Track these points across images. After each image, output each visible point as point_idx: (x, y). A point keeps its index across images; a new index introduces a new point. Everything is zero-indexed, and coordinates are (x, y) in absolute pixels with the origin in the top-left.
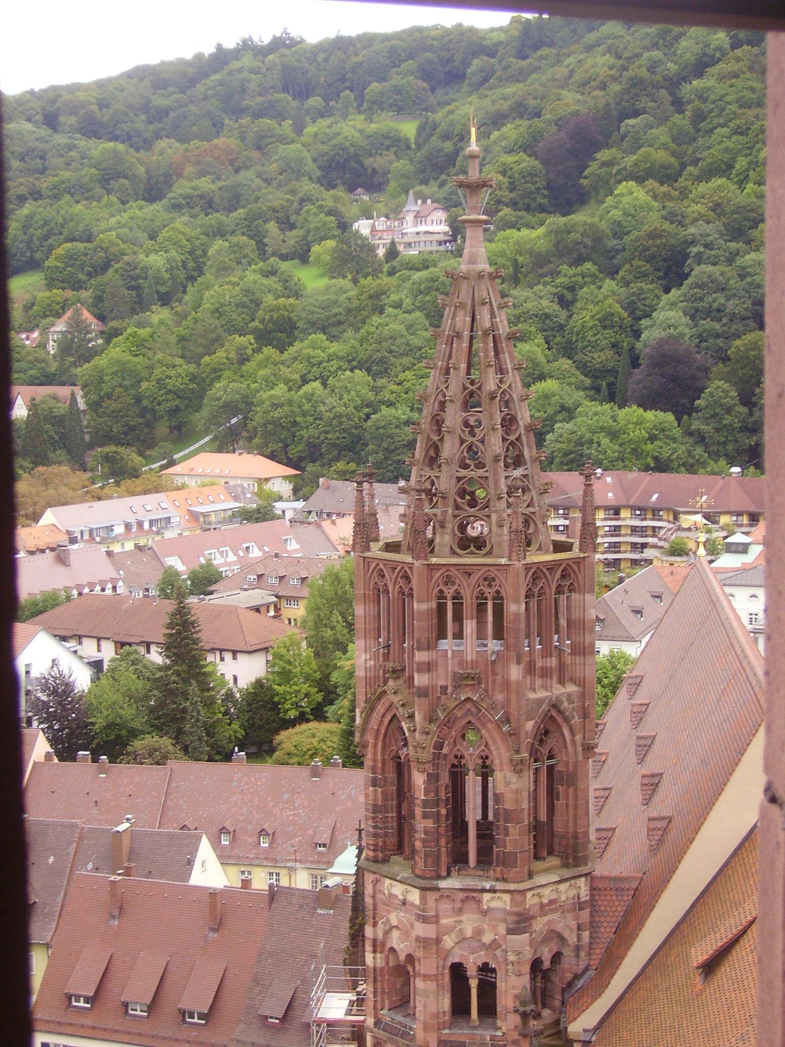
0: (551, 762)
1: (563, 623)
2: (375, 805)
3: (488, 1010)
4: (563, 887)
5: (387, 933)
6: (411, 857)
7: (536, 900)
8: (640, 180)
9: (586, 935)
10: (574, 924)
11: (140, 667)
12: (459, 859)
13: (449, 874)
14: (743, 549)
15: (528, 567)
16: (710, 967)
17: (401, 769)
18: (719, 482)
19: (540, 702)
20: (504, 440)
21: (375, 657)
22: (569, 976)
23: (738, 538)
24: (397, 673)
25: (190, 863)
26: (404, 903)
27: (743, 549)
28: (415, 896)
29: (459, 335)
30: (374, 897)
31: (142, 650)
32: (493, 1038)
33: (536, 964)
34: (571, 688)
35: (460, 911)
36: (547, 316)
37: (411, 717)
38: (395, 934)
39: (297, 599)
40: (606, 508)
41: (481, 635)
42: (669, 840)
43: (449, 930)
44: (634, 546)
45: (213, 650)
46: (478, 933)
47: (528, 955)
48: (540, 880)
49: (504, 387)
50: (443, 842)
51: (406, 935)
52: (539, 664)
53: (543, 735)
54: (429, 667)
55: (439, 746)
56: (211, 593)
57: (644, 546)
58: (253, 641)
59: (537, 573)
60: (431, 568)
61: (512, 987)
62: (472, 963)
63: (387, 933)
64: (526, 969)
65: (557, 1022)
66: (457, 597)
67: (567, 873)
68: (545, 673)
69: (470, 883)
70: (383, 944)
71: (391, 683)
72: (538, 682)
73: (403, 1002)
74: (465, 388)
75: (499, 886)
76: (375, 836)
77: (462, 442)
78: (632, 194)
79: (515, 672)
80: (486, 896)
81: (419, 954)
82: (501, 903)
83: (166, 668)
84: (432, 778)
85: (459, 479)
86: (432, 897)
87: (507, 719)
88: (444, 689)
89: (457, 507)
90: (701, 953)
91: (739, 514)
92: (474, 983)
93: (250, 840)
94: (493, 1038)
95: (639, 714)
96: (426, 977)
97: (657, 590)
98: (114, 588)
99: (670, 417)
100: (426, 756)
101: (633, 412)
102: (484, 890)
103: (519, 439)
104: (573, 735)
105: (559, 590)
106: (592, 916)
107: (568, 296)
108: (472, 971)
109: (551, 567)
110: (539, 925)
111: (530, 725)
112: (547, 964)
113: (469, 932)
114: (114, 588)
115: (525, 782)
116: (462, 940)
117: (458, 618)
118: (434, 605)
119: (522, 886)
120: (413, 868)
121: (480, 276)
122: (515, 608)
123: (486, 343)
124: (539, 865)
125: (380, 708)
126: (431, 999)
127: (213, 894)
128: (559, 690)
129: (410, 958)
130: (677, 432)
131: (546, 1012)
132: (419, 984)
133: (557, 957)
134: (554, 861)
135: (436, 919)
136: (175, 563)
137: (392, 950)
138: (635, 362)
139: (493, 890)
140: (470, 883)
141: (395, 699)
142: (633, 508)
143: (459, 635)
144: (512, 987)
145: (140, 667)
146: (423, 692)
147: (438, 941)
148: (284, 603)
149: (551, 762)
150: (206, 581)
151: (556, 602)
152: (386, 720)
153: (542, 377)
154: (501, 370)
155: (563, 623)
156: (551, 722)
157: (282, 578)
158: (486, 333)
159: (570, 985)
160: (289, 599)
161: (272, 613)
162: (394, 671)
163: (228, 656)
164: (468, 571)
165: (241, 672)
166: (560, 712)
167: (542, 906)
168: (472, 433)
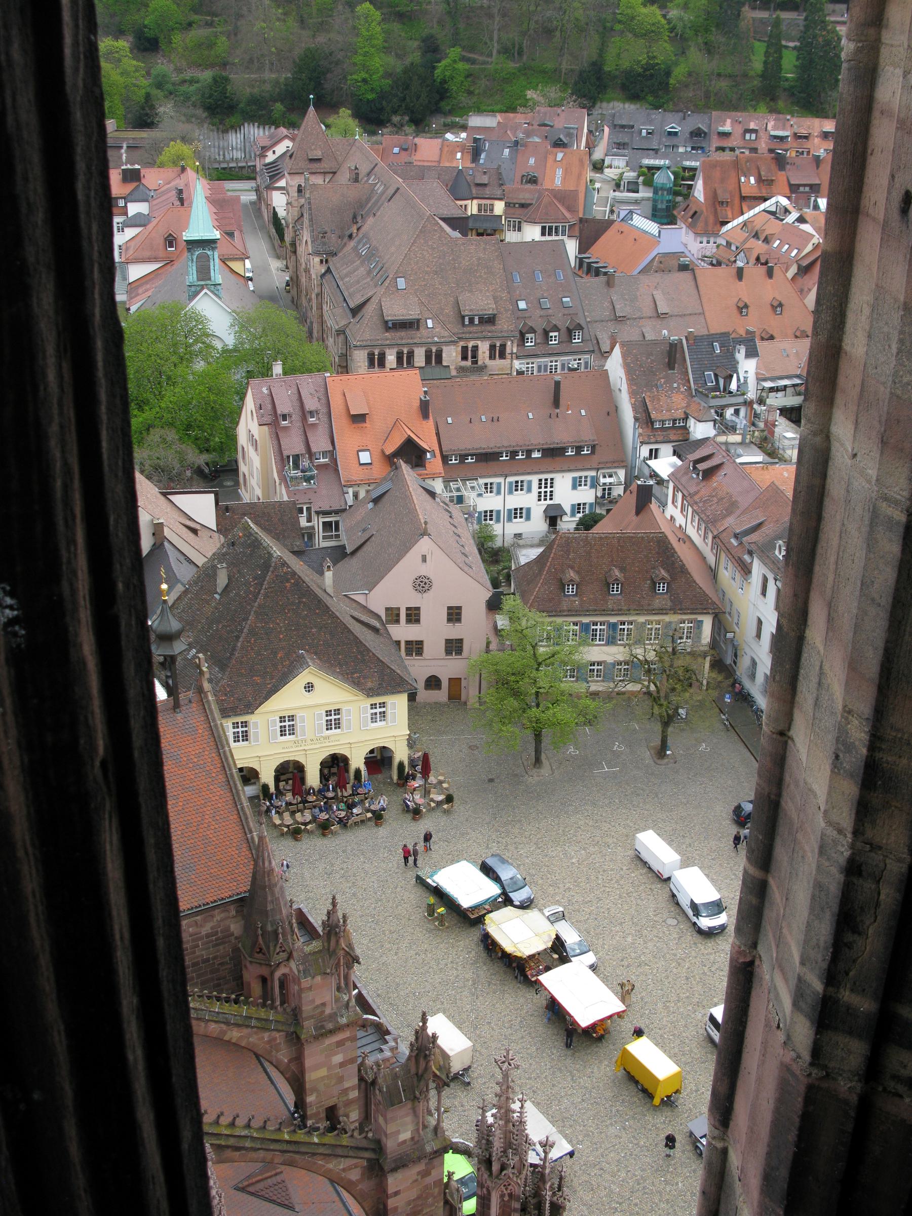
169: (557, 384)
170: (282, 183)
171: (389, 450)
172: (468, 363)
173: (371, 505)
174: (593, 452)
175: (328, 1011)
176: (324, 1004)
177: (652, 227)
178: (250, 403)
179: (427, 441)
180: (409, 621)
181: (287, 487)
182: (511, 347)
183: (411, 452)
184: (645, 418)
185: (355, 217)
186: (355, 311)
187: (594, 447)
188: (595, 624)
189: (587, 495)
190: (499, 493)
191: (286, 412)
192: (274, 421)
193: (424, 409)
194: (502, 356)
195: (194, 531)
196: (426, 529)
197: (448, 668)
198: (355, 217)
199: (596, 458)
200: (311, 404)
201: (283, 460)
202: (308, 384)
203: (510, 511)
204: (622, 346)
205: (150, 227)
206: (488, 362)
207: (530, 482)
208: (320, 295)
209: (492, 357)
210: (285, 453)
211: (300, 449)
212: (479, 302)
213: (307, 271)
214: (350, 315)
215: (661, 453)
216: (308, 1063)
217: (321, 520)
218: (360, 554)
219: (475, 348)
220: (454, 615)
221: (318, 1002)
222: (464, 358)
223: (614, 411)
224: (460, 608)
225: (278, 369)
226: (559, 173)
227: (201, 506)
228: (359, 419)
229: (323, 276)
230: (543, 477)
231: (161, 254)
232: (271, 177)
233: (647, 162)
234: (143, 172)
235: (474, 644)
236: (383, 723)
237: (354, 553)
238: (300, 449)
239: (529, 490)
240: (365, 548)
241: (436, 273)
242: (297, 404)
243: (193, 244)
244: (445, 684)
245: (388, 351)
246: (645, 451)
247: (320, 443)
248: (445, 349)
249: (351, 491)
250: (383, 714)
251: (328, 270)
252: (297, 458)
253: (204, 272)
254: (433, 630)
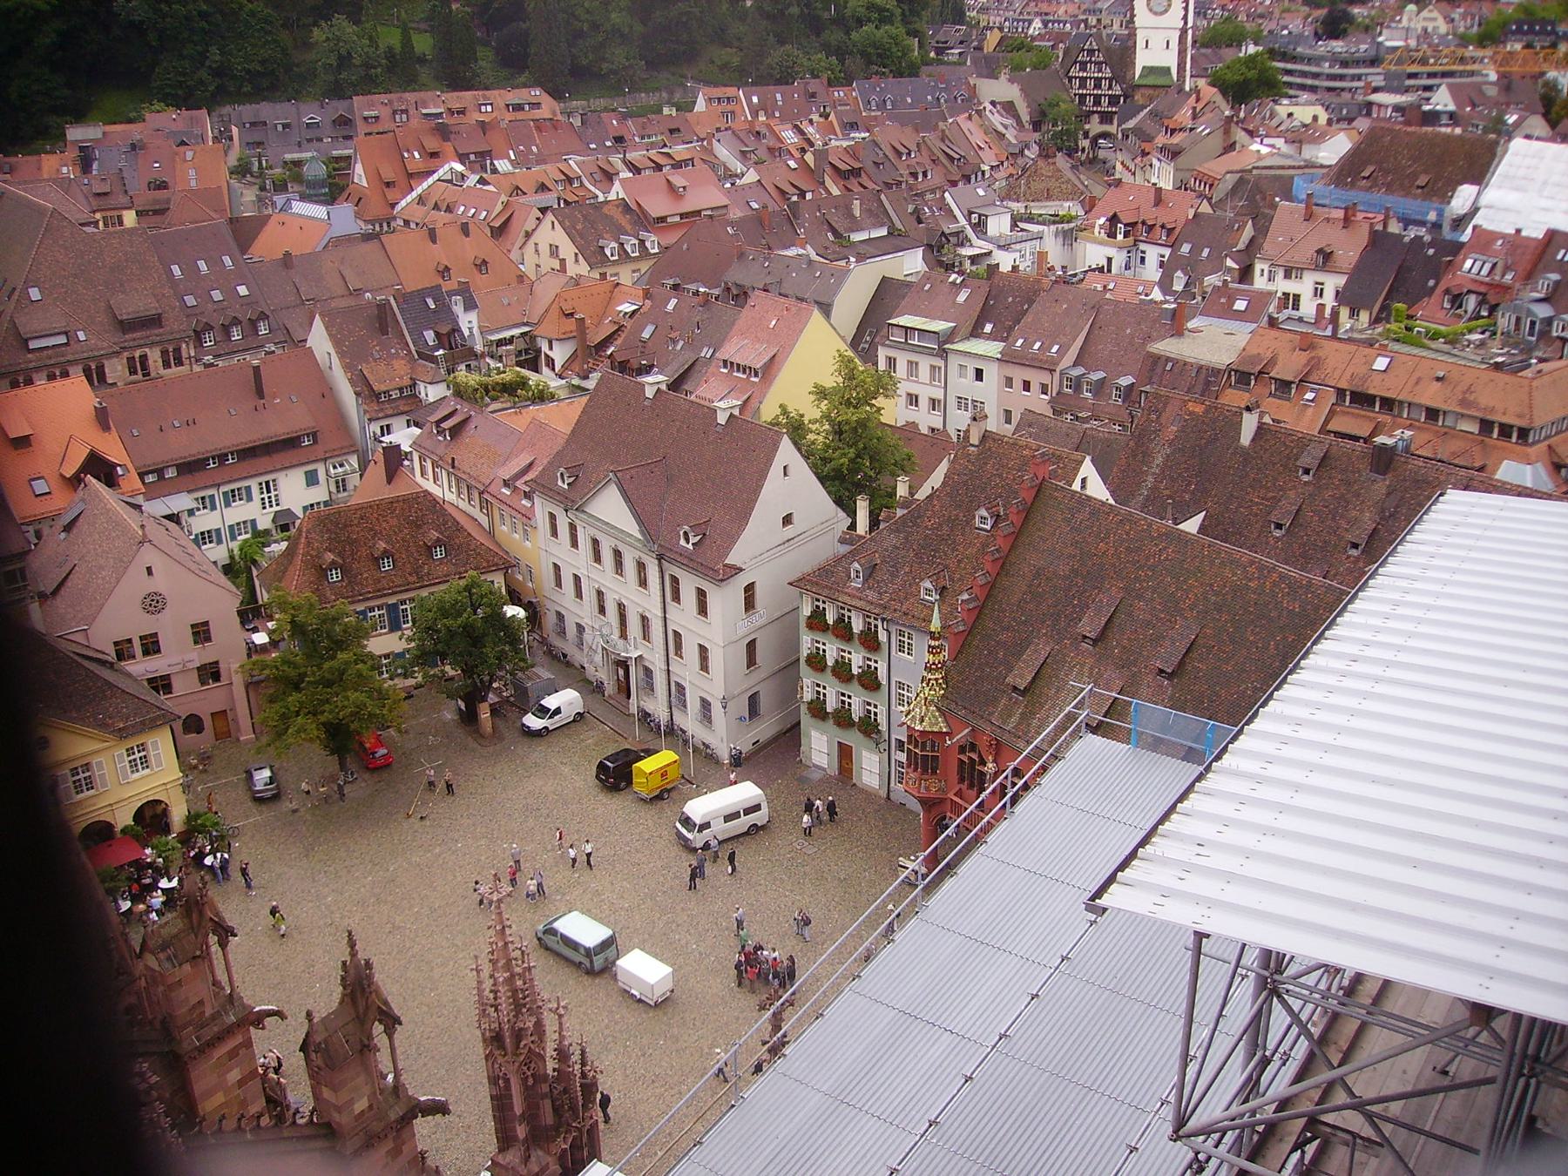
169: (256, 369)
171: (69, 472)
172: (140, 376)
173: (63, 535)
174: (315, 441)
175: (208, 1012)
176: (201, 1003)
177: (319, 211)
179: (114, 451)
180: (146, 653)
182: (188, 350)
183: (100, 468)
184: (368, 393)
187: (314, 435)
188: (372, 609)
189: (319, 494)
190: (213, 508)
193: (102, 418)
194: (179, 363)
196: (144, 535)
197: (207, 702)
199: (320, 450)
203: (231, 527)
204: (322, 316)
206: (162, 372)
207: (248, 489)
209: (167, 365)
212: (135, 304)
215: (394, 428)
216: (198, 1088)
219: (144, 358)
220: (201, 633)
221: (194, 1001)
222: (133, 371)
223: (327, 392)
224: (206, 623)
226: (192, 172)
230: (263, 479)
233: (288, 157)
235: (233, 665)
236: (147, 771)
239: (250, 499)
241: (75, 276)
244: (208, 722)
245: (34, 376)
246: (375, 428)
248: (106, 363)
250: (145, 761)
254: (178, 656)
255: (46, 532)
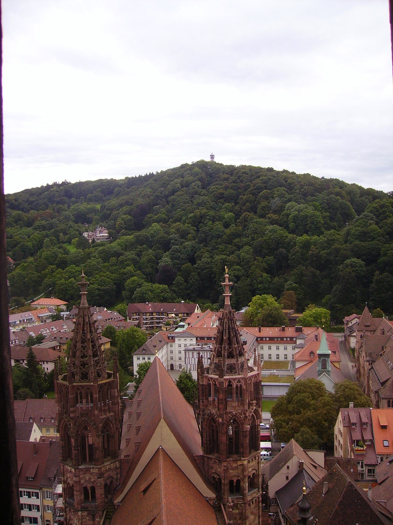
0: (107, 433)
1: (109, 397)
2: (62, 446)
3: (94, 497)
4: (112, 465)
5: (67, 479)
6: (72, 459)
7: (105, 469)
8: (158, 222)
9: (119, 476)
10: (115, 473)
11: (20, 368)
12: (84, 460)
13: (82, 464)
14: (183, 326)
15: (99, 385)
16: (145, 491)
17: (69, 438)
18: (178, 305)
19: (104, 418)
20: (92, 350)
21: (61, 408)
22: (115, 486)
23: (182, 323)
24: (66, 413)
25: (31, 431)
26: (71, 471)
27: (183, 326)
28: (73, 470)
29: (80, 324)
30: (63, 470)
31: (21, 362)
32: (95, 505)
33: (106, 485)
34: (112, 414)
35: (85, 474)
36: (134, 259)
37: (70, 424)
38: (69, 479)
39: (65, 344)
40: (149, 313)
41: (87, 402)
42: (140, 448)
43: (82, 479)
44: (157, 322)
45: (41, 361)
46: (90, 479)
47: (103, 483)
48: (106, 464)
49: (92, 336)
50: (80, 456)
51: (72, 480)
52: (103, 408)
53: (104, 427)
54: (73, 412)
55: (77, 432)
56: (42, 343)
57: (160, 322)
58: (52, 358)
59: (101, 386)
60: (74, 386)
61: (100, 492)
62: (89, 486)
63: (67, 479)
64: (103, 487)
65: (112, 499)
66: (81, 393)
67: (113, 461)
68: (105, 411)
69: (87, 466)
70: (66, 481)
71: (65, 415)
72: (103, 413)
73: (72, 496)
74: (82, 337)
75: (95, 467)
76: (63, 454)
77: (82, 352)
78: (156, 226)
79: (96, 412)
80: (91, 470)
81: (75, 485)
82: (96, 471)
83: (27, 369)
84: (76, 440)
85: (81, 361)
86: (77, 471)
87: (95, 424)
88: (78, 417)
89: (81, 369)
90: (142, 487)
91: (184, 313)
92: (90, 491)
93: (48, 420)
94: (95, 505)
95: (139, 403)
96: (77, 491)
97: (160, 340)
98: (15, 342)
99: (166, 286)
100: (74, 435)
101: (156, 285)
102: (91, 468)
103: (97, 350)
104: (113, 425)
105: (108, 389)
106: (120, 470)
107: (140, 254)
108: (89, 488)
109: (105, 384)
110: (106, 475)
111: (101, 425)
112: (109, 484)
113: (88, 479)
114: (15, 342)
115: (101, 439)
116: (86, 481)
117: (81, 398)
118: (75, 395)
119: (100, 466)
120: (73, 462)
121: (85, 308)
122: (96, 396)
123: (87, 325)
124: (105, 459)
125: (62, 422)
126: (78, 496)
127: (34, 444)
128: (109, 415)
129: (73, 485)
130: (168, 290)
131: (109, 496)
132: (75, 493)
133: (111, 482)
134: (110, 458)
135: (79, 476)
136: (32, 334)
137: (68, 483)
138: (157, 271)
139: (93, 468)
140: (87, 466)
141: (66, 420)
142: (156, 313)
143: (81, 402)
144: (100, 492)
145: (20, 368)
146: (72, 418)
147: (80, 481)
148: (62, 345)
149: (107, 433)
150: (40, 339)
151: (107, 392)
152: (64, 424)
153: (133, 276)
154: (91, 332)
155: (109, 397)
156: (107, 423)
157: (61, 338)
158: (87, 323)
159: (115, 489)
160: (63, 344)
161: (58, 348)
162: (65, 412)
163: (45, 363)
164: (83, 387)
165: (49, 367)
166: (109, 420)
167: (106, 470)
168: (84, 349)
170: (355, 334)
173: (388, 464)
178: (340, 418)
181: (353, 453)
185: (383, 347)
186: (383, 384)
191: (354, 422)
192: (349, 426)
195: (315, 467)
198: (383, 347)
200: (364, 420)
201: (352, 442)
202: (363, 412)
205: (304, 349)
208: (368, 377)
210: (353, 439)
211: (359, 438)
213: (364, 368)
214: (380, 385)
217: (367, 468)
218: (383, 484)
225: (351, 405)
227: (319, 457)
228: (384, 427)
229: (370, 370)
231: (308, 358)
232: (350, 332)
234: (303, 328)
237: (380, 484)
238: (359, 438)
240: (385, 482)
242: (359, 419)
243: (320, 356)
247: (367, 436)
249: (380, 457)
251: (372, 368)
252: (358, 441)
253: (324, 366)
255: (384, 459)
